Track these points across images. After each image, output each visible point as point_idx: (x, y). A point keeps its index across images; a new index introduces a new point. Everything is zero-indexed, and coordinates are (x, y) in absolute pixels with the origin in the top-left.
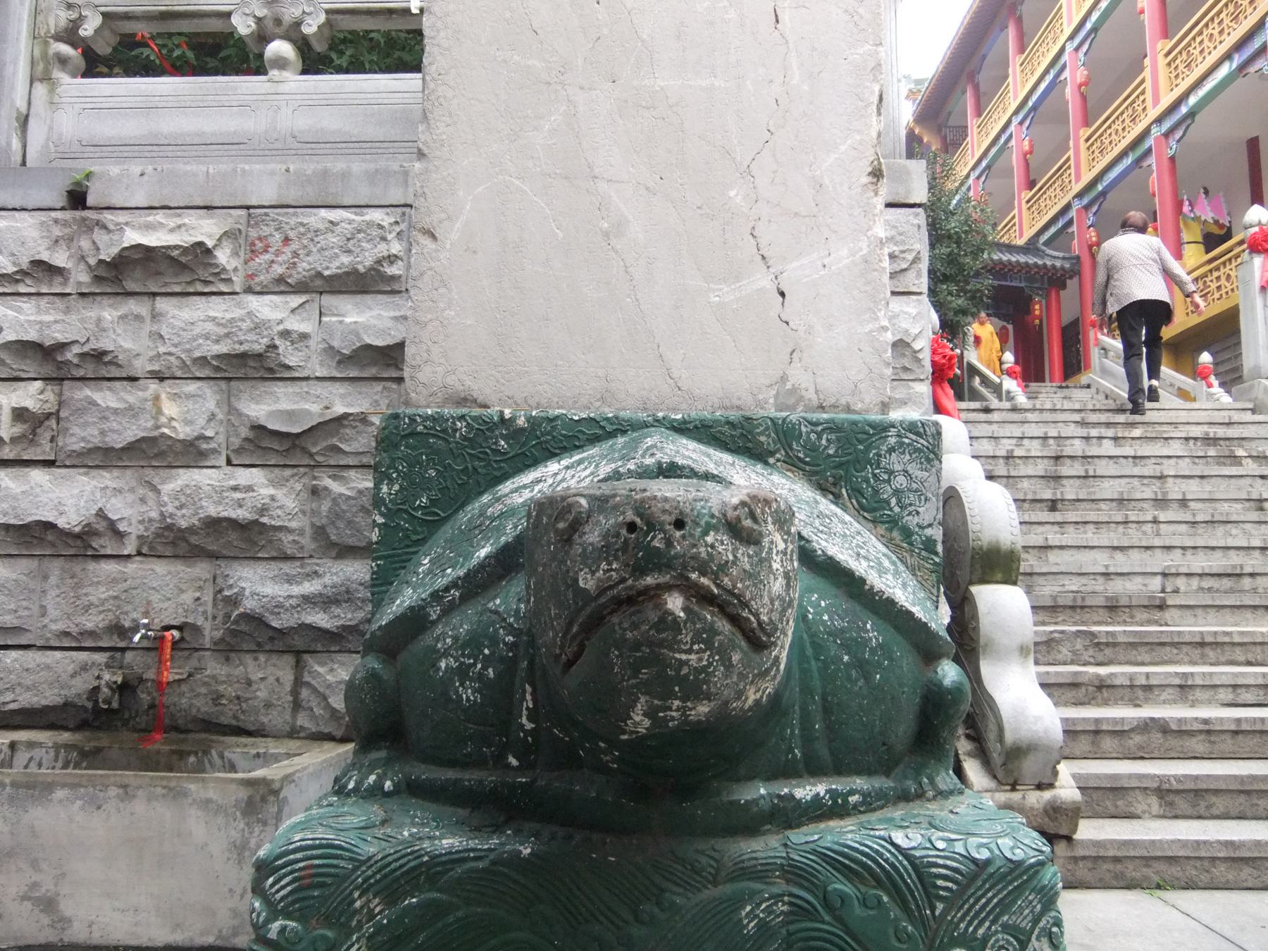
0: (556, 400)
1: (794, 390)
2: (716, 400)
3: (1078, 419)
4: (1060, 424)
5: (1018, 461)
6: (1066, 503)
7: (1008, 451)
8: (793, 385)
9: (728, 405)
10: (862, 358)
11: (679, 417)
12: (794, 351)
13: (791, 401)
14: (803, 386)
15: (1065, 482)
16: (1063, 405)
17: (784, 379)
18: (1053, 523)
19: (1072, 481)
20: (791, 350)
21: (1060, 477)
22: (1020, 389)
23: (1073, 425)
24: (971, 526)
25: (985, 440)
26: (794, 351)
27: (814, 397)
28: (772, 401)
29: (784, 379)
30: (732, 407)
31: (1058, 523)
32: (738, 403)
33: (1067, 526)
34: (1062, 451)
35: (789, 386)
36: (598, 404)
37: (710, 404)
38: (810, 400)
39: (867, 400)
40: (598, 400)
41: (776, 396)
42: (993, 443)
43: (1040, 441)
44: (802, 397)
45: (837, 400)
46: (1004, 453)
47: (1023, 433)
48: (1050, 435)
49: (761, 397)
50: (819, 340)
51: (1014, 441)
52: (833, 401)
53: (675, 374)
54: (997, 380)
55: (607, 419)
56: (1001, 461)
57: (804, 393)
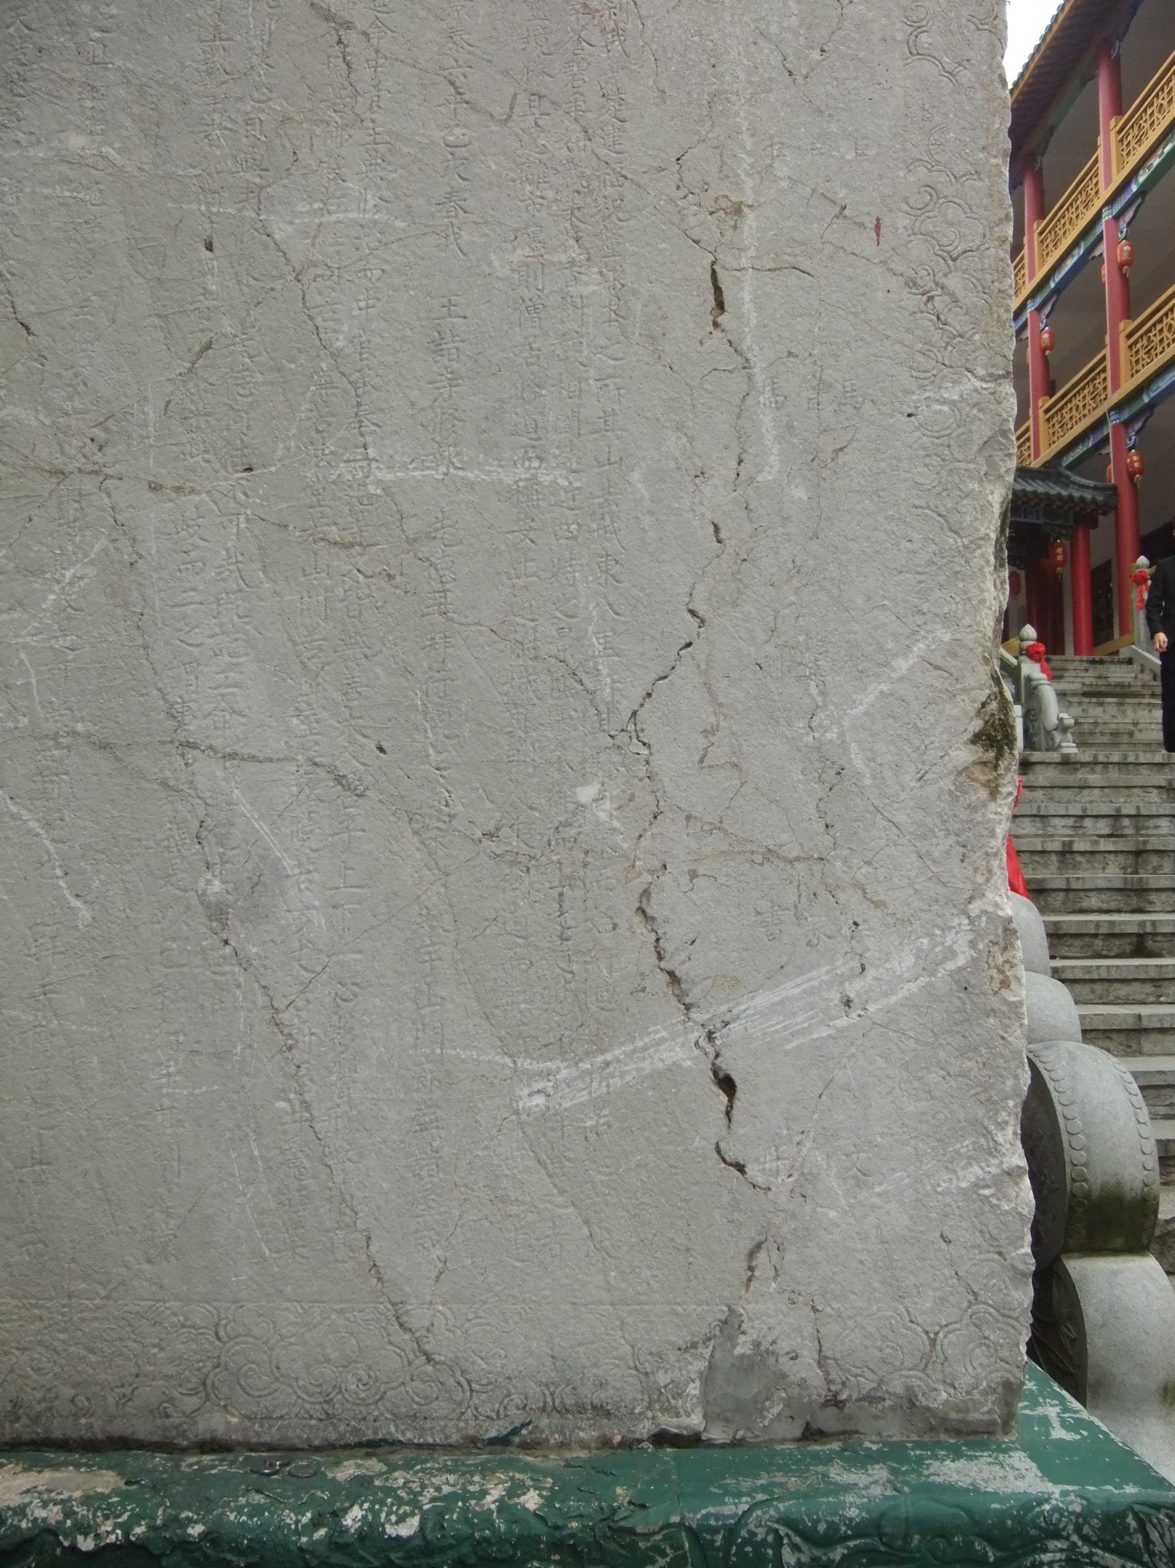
0: (68, 1392)
1: (761, 1355)
2: (534, 1390)
3: (1163, 784)
4: (1136, 790)
5: (1079, 858)
6: (1159, 938)
7: (1064, 843)
8: (757, 1345)
9: (569, 1401)
10: (952, 1263)
11: (408, 1529)
12: (759, 1246)
13: (750, 1390)
14: (784, 1346)
15: (1153, 897)
16: (1137, 756)
17: (730, 1325)
18: (1144, 981)
19: (1164, 896)
20: (747, 1245)
21: (1146, 890)
22: (1044, 676)
23: (1155, 791)
24: (1068, 1154)
25: (1027, 820)
26: (759, 1246)
27: (815, 1376)
28: (694, 1389)
29: (730, 1325)
30: (581, 1409)
31: (1152, 980)
32: (600, 1396)
33: (1166, 984)
34: (1145, 843)
35: (743, 1348)
36: (192, 1402)
37: (517, 1400)
38: (803, 1384)
39: (965, 1381)
40: (193, 1393)
41: (707, 1378)
42: (1039, 825)
43: (1110, 821)
44: (783, 1376)
45: (881, 1382)
46: (1056, 846)
47: (1084, 810)
48: (1124, 812)
49: (662, 1379)
50: (832, 1214)
51: (1070, 822)
52: (867, 1385)
53: (418, 1317)
54: (1014, 662)
55: (184, 1545)
56: (1054, 858)
57: (785, 1364)
